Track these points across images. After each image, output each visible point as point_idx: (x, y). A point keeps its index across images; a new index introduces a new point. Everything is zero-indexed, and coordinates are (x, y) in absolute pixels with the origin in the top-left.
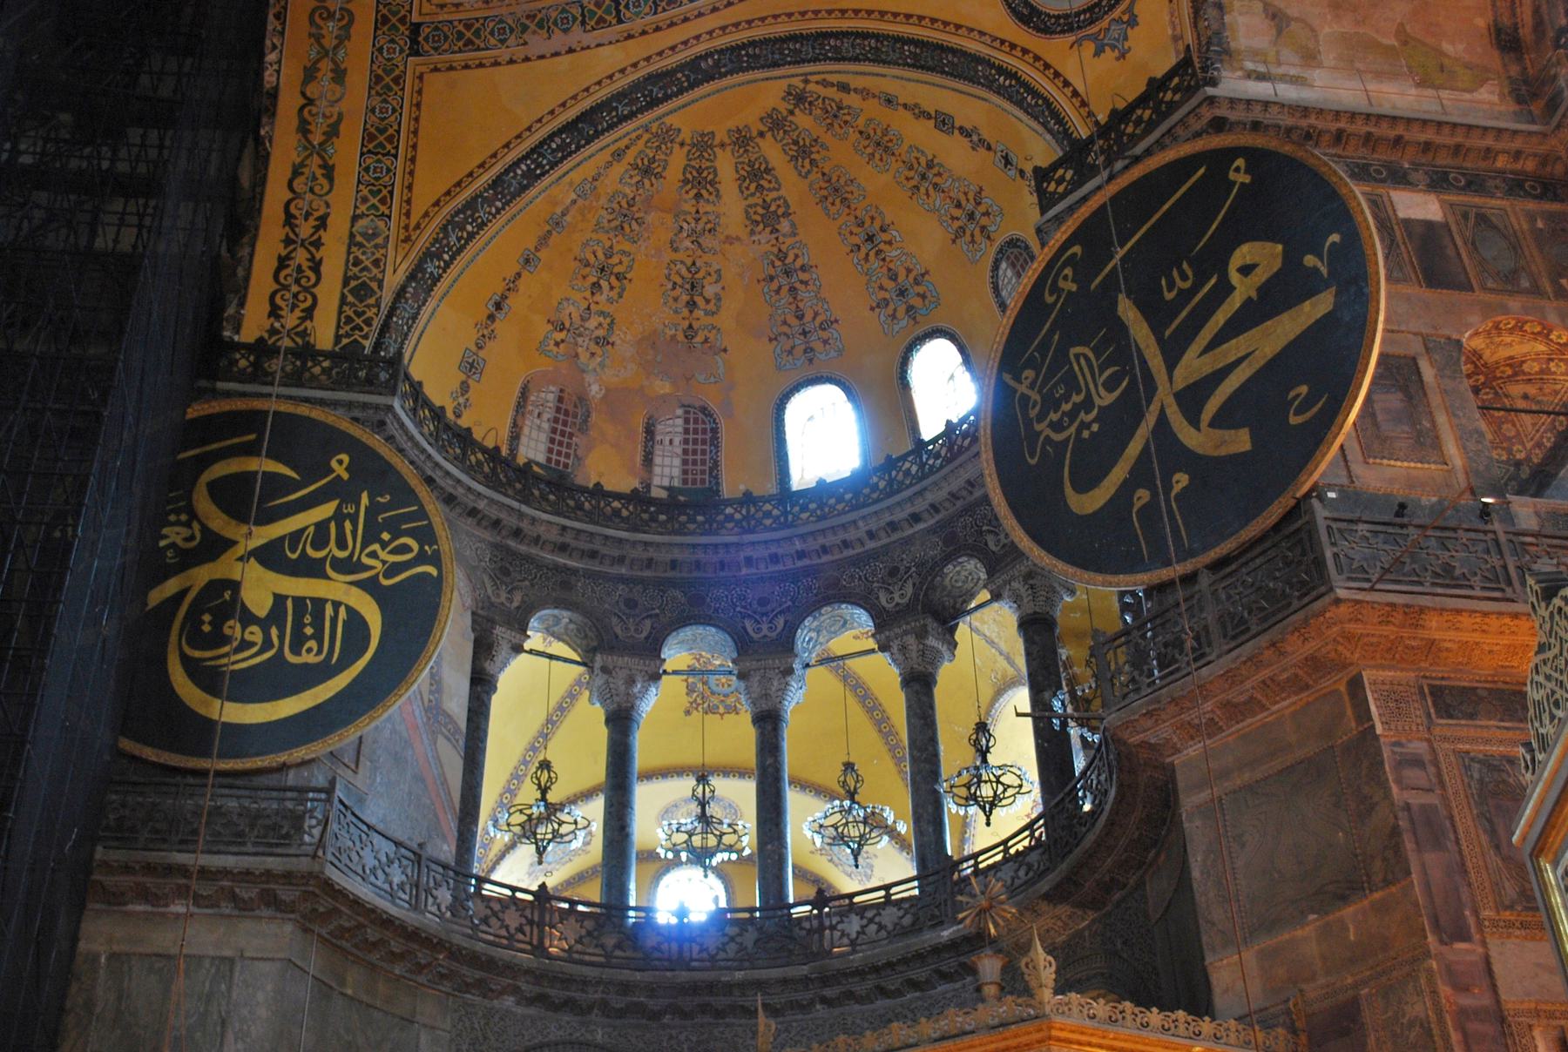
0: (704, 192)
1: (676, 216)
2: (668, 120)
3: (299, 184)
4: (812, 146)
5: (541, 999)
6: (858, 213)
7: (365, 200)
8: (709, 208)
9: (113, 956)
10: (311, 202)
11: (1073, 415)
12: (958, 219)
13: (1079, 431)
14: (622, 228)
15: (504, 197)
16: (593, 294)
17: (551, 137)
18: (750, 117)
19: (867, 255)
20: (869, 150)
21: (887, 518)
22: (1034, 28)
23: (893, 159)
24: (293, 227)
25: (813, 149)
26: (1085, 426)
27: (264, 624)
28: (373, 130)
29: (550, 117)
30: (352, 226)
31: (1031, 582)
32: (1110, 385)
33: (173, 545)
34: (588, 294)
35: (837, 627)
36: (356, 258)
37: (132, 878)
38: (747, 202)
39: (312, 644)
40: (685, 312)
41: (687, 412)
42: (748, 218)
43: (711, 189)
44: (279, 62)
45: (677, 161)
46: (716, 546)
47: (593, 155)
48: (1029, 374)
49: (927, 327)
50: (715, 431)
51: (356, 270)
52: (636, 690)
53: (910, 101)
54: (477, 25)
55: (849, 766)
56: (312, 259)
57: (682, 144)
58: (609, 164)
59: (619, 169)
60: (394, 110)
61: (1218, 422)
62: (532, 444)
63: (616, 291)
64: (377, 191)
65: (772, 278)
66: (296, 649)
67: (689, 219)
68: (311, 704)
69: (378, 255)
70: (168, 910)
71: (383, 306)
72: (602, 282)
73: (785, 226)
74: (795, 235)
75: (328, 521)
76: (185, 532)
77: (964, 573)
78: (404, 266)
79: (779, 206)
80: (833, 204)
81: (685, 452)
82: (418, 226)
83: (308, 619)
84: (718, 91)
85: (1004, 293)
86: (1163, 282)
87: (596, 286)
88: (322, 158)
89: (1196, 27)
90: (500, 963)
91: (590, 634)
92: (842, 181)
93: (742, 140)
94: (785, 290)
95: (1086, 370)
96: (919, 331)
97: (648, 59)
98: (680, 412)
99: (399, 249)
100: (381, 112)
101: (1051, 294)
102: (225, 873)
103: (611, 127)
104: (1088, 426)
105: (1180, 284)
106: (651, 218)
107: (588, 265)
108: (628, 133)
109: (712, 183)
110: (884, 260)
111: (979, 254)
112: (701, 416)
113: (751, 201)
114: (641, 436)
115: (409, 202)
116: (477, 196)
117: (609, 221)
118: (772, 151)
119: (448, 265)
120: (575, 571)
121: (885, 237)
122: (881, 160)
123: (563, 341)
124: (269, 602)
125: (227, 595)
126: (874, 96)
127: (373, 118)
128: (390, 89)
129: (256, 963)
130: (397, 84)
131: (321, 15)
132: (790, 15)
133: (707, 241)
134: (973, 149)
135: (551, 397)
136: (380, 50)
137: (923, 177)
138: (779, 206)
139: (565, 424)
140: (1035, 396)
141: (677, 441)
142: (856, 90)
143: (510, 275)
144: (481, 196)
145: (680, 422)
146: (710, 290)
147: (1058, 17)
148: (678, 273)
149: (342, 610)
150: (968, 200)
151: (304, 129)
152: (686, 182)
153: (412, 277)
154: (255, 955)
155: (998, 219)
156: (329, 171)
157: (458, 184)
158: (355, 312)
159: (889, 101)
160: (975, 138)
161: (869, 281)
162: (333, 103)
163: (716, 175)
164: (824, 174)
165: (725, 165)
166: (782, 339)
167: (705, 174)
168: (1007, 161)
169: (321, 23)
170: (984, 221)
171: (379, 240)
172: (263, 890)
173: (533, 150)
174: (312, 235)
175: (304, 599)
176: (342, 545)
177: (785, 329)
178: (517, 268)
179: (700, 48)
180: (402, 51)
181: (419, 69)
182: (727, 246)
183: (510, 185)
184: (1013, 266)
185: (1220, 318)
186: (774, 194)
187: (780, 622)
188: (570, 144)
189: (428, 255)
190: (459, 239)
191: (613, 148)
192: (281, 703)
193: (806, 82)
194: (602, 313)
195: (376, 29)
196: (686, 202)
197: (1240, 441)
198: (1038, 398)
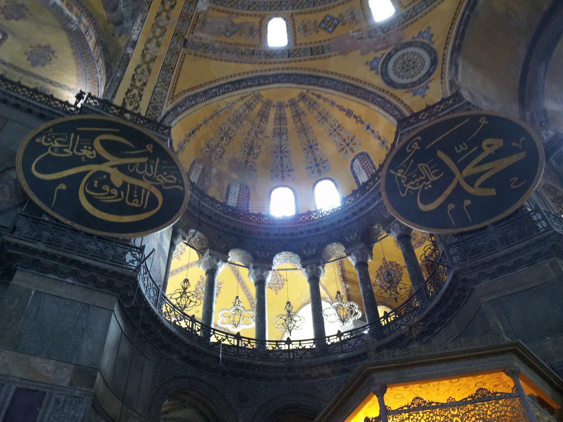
1: (253, 124)
2: (262, 92)
3: (139, 71)
5: (186, 359)
7: (160, 83)
9: (36, 292)
11: (421, 182)
17: (226, 84)
18: (286, 100)
21: (308, 228)
26: (424, 186)
27: (119, 190)
32: (435, 175)
33: (85, 156)
34: (219, 140)
37: (54, 262)
39: (137, 200)
40: (246, 155)
41: (241, 186)
42: (274, 131)
45: (259, 107)
48: (402, 171)
49: (324, 177)
50: (249, 194)
52: (219, 264)
53: (340, 104)
55: (288, 303)
58: (238, 100)
59: (241, 103)
61: (483, 185)
62: (194, 177)
63: (228, 141)
64: (164, 82)
65: (276, 152)
66: (131, 199)
67: (256, 126)
70: (65, 280)
71: (162, 114)
73: (284, 137)
76: (91, 153)
77: (332, 249)
81: (239, 197)
82: (177, 96)
83: (135, 192)
86: (456, 147)
87: (222, 138)
90: (179, 339)
91: (204, 243)
93: (280, 106)
94: (279, 157)
96: (321, 177)
98: (239, 185)
101: (409, 149)
102: (97, 268)
103: (244, 88)
104: (427, 186)
105: (462, 148)
106: (245, 122)
109: (267, 117)
112: (245, 188)
113: (277, 126)
118: (288, 112)
119: (183, 111)
120: (203, 221)
121: (316, 147)
122: (323, 122)
123: (208, 151)
124: (121, 183)
125: (105, 177)
126: (328, 101)
129: (99, 309)
133: (259, 135)
135: (201, 167)
137: (335, 130)
140: (404, 177)
141: (236, 194)
146: (256, 151)
148: (248, 142)
149: (148, 193)
150: (348, 139)
151: (143, 55)
152: (259, 114)
154: (100, 306)
160: (358, 119)
162: (154, 52)
163: (269, 114)
165: (272, 113)
166: (275, 172)
168: (368, 127)
170: (352, 146)
172: (109, 280)
176: (149, 171)
177: (277, 169)
178: (202, 122)
179: (280, 72)
183: (209, 94)
184: (360, 160)
185: (480, 158)
187: (268, 254)
189: (178, 105)
191: (241, 95)
194: (222, 147)
197: (492, 192)
198: (405, 177)
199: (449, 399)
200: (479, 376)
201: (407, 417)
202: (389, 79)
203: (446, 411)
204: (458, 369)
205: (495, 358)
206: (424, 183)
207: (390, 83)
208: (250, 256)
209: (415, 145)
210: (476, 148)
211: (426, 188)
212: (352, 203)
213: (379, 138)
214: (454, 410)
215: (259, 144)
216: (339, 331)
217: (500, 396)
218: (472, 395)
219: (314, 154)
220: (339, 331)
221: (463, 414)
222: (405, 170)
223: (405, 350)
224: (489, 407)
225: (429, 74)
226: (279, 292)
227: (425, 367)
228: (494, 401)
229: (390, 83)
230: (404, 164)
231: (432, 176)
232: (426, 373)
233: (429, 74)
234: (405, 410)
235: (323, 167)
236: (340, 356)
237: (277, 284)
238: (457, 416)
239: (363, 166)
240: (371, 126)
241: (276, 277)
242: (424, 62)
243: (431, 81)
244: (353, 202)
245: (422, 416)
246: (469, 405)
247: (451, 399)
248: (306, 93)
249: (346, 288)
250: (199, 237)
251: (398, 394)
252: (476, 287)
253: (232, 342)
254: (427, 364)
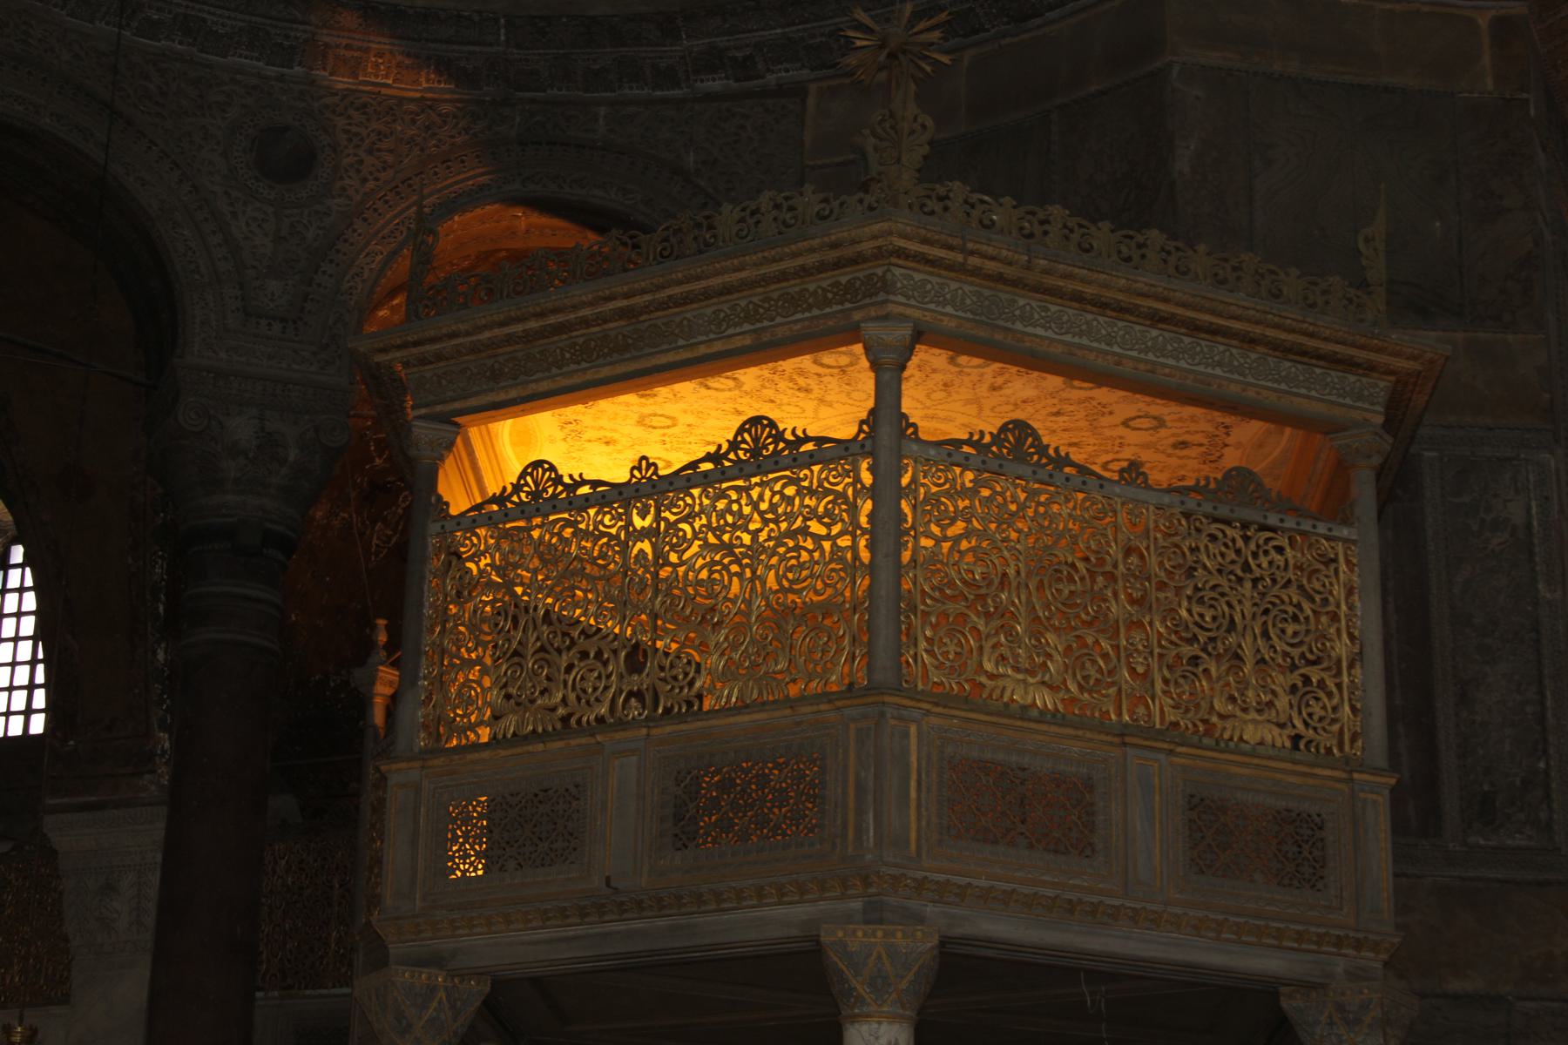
232: (1085, 341)
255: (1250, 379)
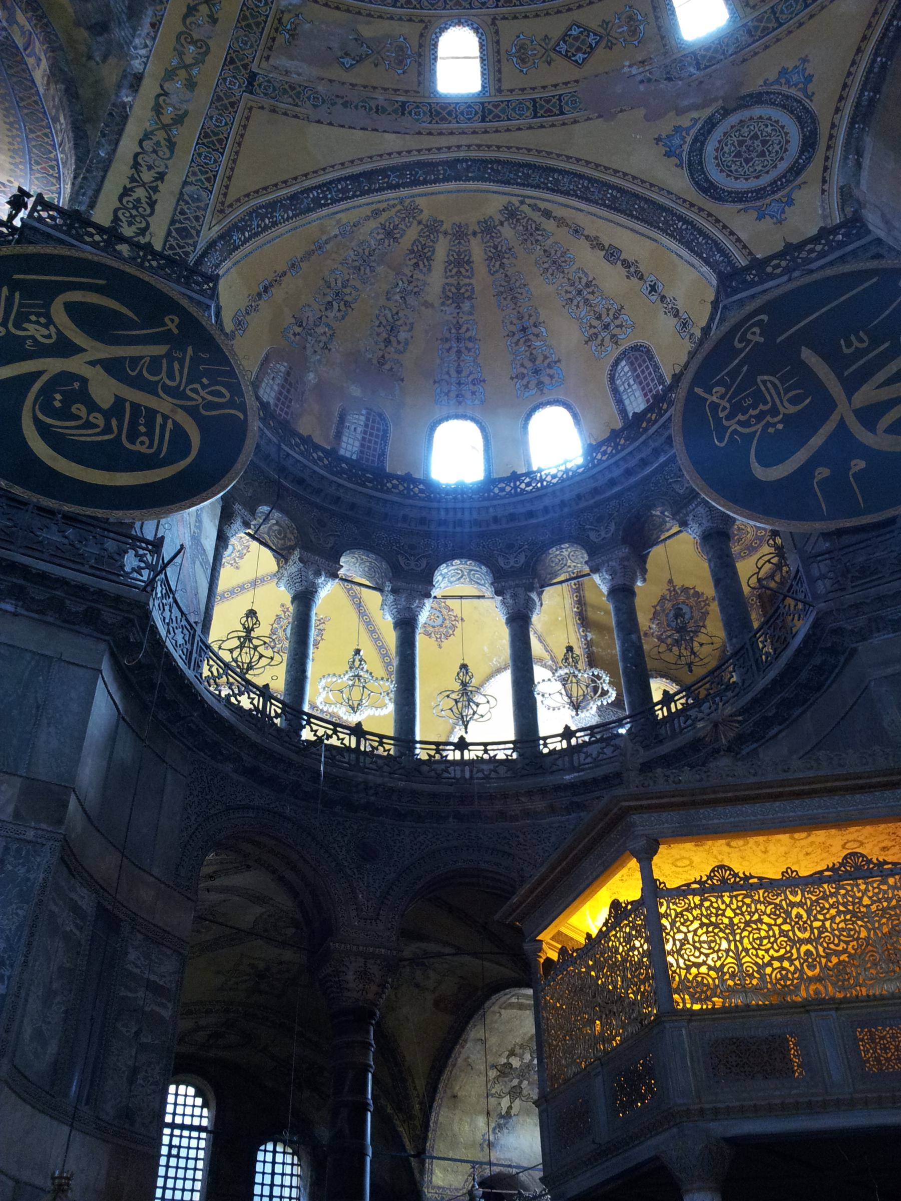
0: (421, 263)
1: (397, 274)
2: (418, 200)
4: (506, 253)
6: (521, 310)
7: (194, 174)
8: (421, 276)
10: (154, 160)
11: (760, 417)
12: (595, 327)
13: (765, 428)
14: (359, 270)
15: (295, 209)
16: (326, 309)
17: (339, 180)
18: (472, 219)
19: (519, 340)
20: (546, 265)
22: (710, 196)
23: (562, 275)
24: (138, 172)
25: (506, 256)
26: (768, 424)
27: (107, 415)
28: (208, 131)
29: (340, 167)
30: (183, 187)
31: (626, 563)
32: (794, 401)
33: (33, 338)
35: (454, 579)
36: (182, 209)
38: (447, 281)
40: (382, 345)
41: (368, 413)
42: (444, 292)
43: (426, 263)
44: (148, 57)
45: (412, 233)
46: (386, 501)
47: (360, 206)
48: (721, 390)
50: (386, 432)
51: (182, 217)
53: (593, 234)
54: (298, 89)
55: (464, 667)
56: (150, 198)
57: (420, 223)
58: (368, 218)
59: (373, 224)
60: (226, 124)
62: (268, 390)
63: (342, 313)
65: (447, 340)
66: (132, 438)
67: (405, 280)
68: (141, 482)
69: (198, 214)
71: (198, 247)
72: (334, 303)
73: (466, 306)
74: (470, 314)
75: (162, 357)
78: (216, 228)
79: (467, 290)
80: (505, 299)
81: (364, 439)
82: (231, 206)
83: (142, 421)
84: (458, 191)
85: (618, 382)
86: (842, 342)
88: (168, 135)
89: (843, 210)
92: (518, 284)
93: (460, 234)
95: (773, 391)
97: (419, 151)
98: (364, 412)
99: (215, 216)
100: (216, 121)
101: (740, 341)
102: (63, 582)
105: (856, 344)
106: (381, 269)
107: (329, 287)
108: (389, 200)
109: (429, 259)
110: (529, 346)
111: (604, 354)
112: (378, 419)
113: (450, 281)
114: (336, 419)
115: (227, 187)
116: (277, 201)
117: (353, 261)
118: (477, 249)
119: (246, 240)
120: (287, 489)
121: (535, 330)
123: (299, 334)
124: (112, 400)
125: (76, 385)
126: (567, 225)
127: (210, 122)
128: (227, 109)
130: (232, 107)
131: (186, 38)
132: (529, 150)
133: (411, 300)
134: (628, 277)
135: (283, 369)
136: (225, 79)
137: (579, 293)
138: (467, 290)
139: (288, 391)
140: (724, 403)
141: (359, 430)
142: (555, 218)
143: (280, 271)
144: (281, 202)
145: (363, 418)
146: (403, 336)
147: (731, 192)
148: (385, 316)
149: (170, 425)
150: (608, 315)
151: (158, 109)
152: (412, 251)
153: (221, 237)
155: (629, 330)
156: (172, 145)
157: (265, 188)
158: (177, 244)
159: (576, 231)
161: (514, 359)
162: (182, 102)
164: (506, 276)
165: (442, 250)
167: (426, 251)
168: (653, 288)
169: (185, 45)
171: (202, 205)
173: (324, 185)
174: (152, 182)
175: (140, 405)
176: (171, 376)
178: (285, 268)
179: (462, 154)
180: (240, 86)
181: (250, 104)
182: (423, 308)
183: (302, 203)
184: (632, 364)
186: (467, 281)
187: (424, 563)
188: (350, 190)
190: (259, 226)
191: (374, 206)
192: (118, 475)
193: (522, 202)
194: (328, 325)
195: (224, 64)
196: (407, 266)
198: (728, 406)
199: (787, 872)
200: (853, 829)
201: (698, 902)
202: (707, 180)
203: (778, 895)
204: (810, 812)
205: (888, 793)
206: (769, 418)
207: (708, 188)
208: (384, 565)
209: (754, 333)
210: (887, 345)
211: (771, 430)
212: (608, 459)
213: (676, 315)
214: (795, 894)
215: (411, 320)
216: (567, 728)
217: (891, 870)
218: (834, 864)
219: (529, 346)
220: (567, 728)
221: (812, 902)
222: (728, 389)
223: (700, 770)
224: (867, 890)
225: (796, 170)
226: (445, 643)
227: (740, 807)
228: (879, 878)
229: (708, 188)
230: (727, 374)
231: (786, 404)
232: (741, 818)
233: (796, 170)
234: (694, 890)
235: (549, 375)
236: (567, 777)
237: (441, 626)
238: (800, 904)
239: (638, 376)
240: (660, 288)
241: (441, 612)
242: (787, 142)
243: (799, 187)
244: (612, 455)
245: (728, 903)
246: (825, 886)
247: (789, 871)
248: (517, 204)
249: (586, 639)
250: (277, 523)
251: (684, 858)
252: (861, 646)
253: (346, 742)
254: (745, 800)
255: (839, 809)
